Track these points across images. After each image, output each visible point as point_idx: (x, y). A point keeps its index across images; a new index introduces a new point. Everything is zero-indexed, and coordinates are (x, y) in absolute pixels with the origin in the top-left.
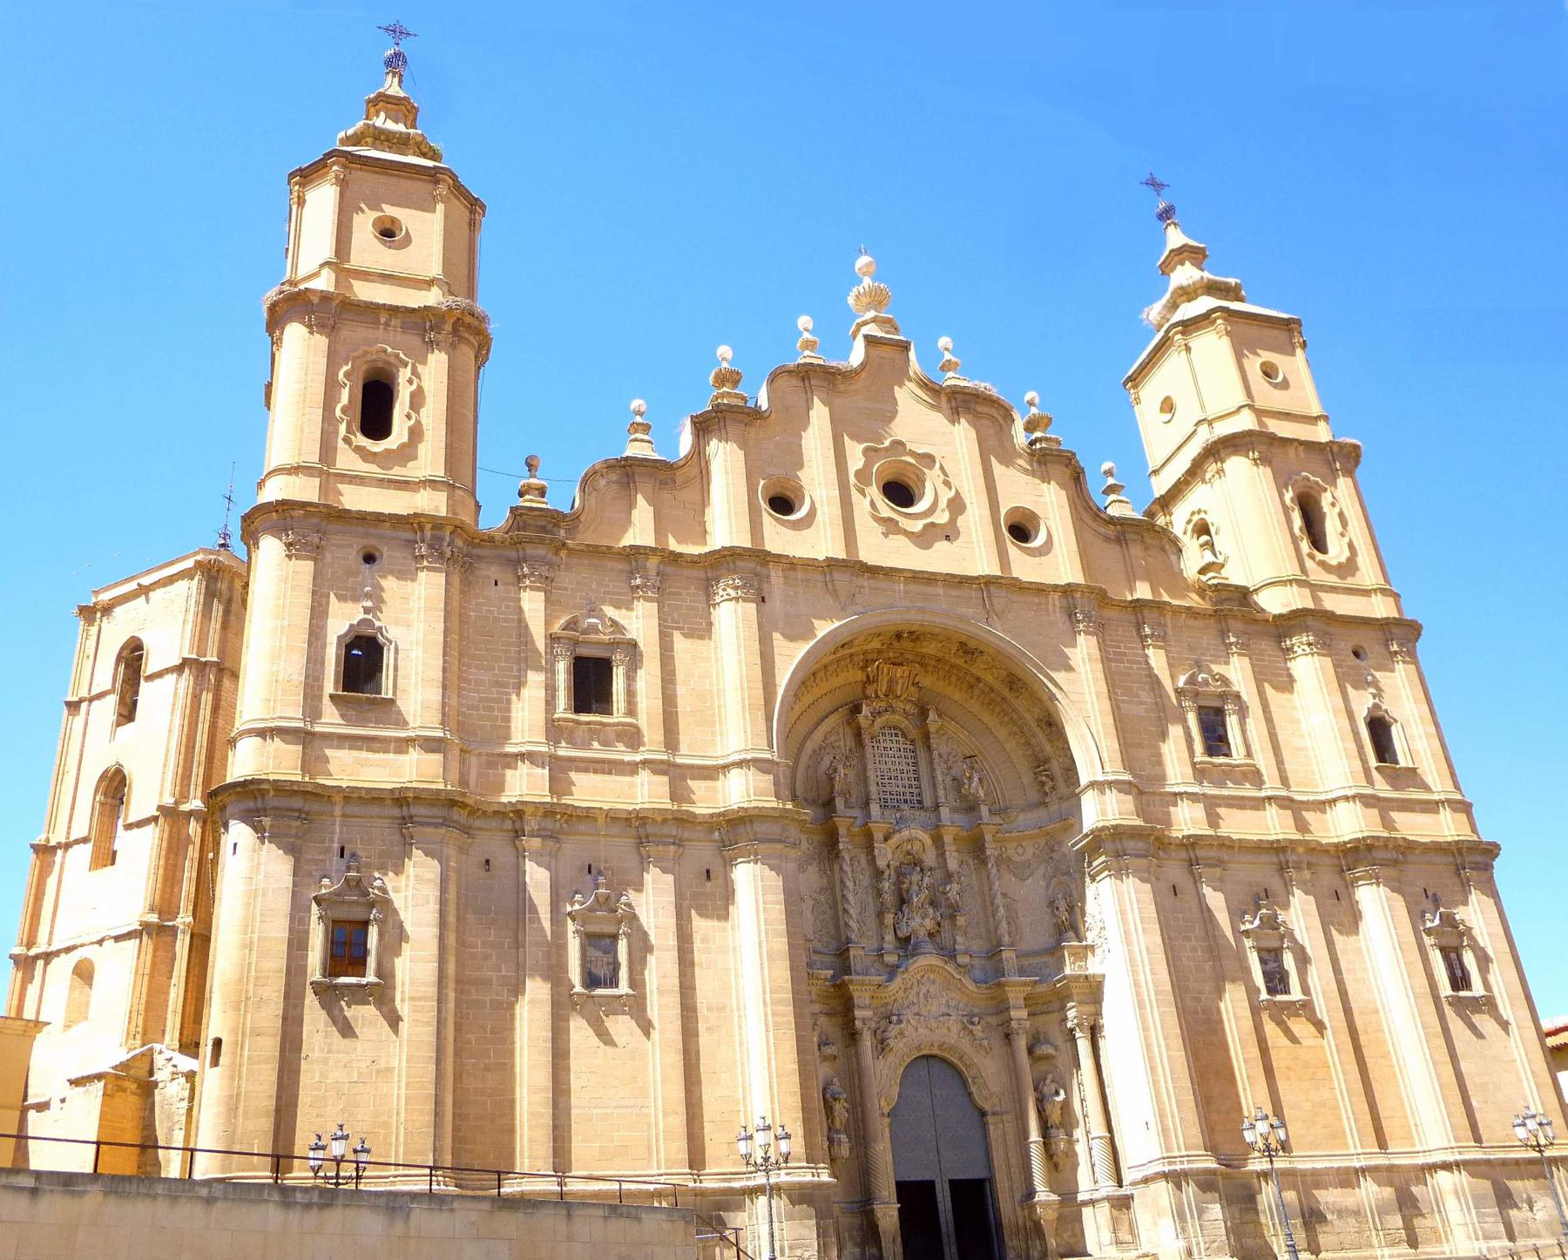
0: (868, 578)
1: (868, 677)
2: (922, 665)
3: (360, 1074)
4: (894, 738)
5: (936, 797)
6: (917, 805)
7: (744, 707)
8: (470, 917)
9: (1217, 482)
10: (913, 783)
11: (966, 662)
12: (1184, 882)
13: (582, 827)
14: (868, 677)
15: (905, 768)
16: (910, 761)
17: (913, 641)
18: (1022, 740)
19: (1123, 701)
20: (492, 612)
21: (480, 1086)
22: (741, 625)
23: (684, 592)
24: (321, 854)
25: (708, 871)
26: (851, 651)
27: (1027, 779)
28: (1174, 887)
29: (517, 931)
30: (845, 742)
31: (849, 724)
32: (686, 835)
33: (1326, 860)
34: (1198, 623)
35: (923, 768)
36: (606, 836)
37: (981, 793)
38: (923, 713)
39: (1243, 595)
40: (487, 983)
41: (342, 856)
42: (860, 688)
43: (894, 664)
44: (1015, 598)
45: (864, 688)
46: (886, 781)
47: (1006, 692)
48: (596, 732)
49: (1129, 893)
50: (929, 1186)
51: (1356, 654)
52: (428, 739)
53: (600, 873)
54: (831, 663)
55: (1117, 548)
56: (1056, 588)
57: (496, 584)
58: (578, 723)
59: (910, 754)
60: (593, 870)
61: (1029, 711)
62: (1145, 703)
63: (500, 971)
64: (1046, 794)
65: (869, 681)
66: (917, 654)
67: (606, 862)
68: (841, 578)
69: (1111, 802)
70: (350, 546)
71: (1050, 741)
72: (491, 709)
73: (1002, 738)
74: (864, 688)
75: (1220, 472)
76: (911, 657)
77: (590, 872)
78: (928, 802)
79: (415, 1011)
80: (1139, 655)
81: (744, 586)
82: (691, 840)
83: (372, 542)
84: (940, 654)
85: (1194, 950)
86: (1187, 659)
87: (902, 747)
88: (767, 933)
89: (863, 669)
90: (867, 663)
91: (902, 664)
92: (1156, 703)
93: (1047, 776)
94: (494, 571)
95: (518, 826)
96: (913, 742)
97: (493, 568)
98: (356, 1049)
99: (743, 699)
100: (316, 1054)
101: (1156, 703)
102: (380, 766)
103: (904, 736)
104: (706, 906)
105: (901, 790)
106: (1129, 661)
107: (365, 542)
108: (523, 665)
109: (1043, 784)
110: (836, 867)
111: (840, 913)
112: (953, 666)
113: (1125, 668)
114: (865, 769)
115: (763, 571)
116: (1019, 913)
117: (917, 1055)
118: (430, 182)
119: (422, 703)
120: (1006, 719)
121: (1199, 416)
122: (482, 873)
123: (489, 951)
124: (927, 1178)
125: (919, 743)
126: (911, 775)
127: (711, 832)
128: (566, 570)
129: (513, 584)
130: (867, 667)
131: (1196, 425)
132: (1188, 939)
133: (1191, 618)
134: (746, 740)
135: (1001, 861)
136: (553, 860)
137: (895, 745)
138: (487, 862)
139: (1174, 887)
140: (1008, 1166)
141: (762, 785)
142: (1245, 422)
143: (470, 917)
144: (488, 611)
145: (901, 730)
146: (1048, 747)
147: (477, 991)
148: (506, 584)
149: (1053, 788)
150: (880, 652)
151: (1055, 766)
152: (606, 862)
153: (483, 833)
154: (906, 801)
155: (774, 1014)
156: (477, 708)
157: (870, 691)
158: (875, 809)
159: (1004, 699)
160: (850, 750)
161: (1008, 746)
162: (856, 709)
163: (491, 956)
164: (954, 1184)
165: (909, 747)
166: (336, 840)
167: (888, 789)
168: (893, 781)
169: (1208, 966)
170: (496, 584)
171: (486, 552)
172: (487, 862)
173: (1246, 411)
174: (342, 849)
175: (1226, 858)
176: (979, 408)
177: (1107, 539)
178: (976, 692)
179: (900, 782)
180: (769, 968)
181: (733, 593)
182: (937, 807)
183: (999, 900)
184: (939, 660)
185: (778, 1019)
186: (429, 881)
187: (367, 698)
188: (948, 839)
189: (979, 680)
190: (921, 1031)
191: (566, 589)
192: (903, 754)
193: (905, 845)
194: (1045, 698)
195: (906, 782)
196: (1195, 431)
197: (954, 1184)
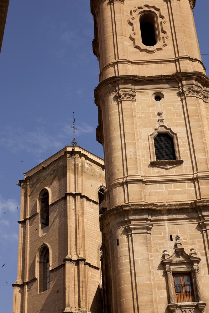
24: (160, 240)
41: (172, 240)
102: (182, 194)
166: (167, 232)
174: (171, 236)
187: (169, 162)
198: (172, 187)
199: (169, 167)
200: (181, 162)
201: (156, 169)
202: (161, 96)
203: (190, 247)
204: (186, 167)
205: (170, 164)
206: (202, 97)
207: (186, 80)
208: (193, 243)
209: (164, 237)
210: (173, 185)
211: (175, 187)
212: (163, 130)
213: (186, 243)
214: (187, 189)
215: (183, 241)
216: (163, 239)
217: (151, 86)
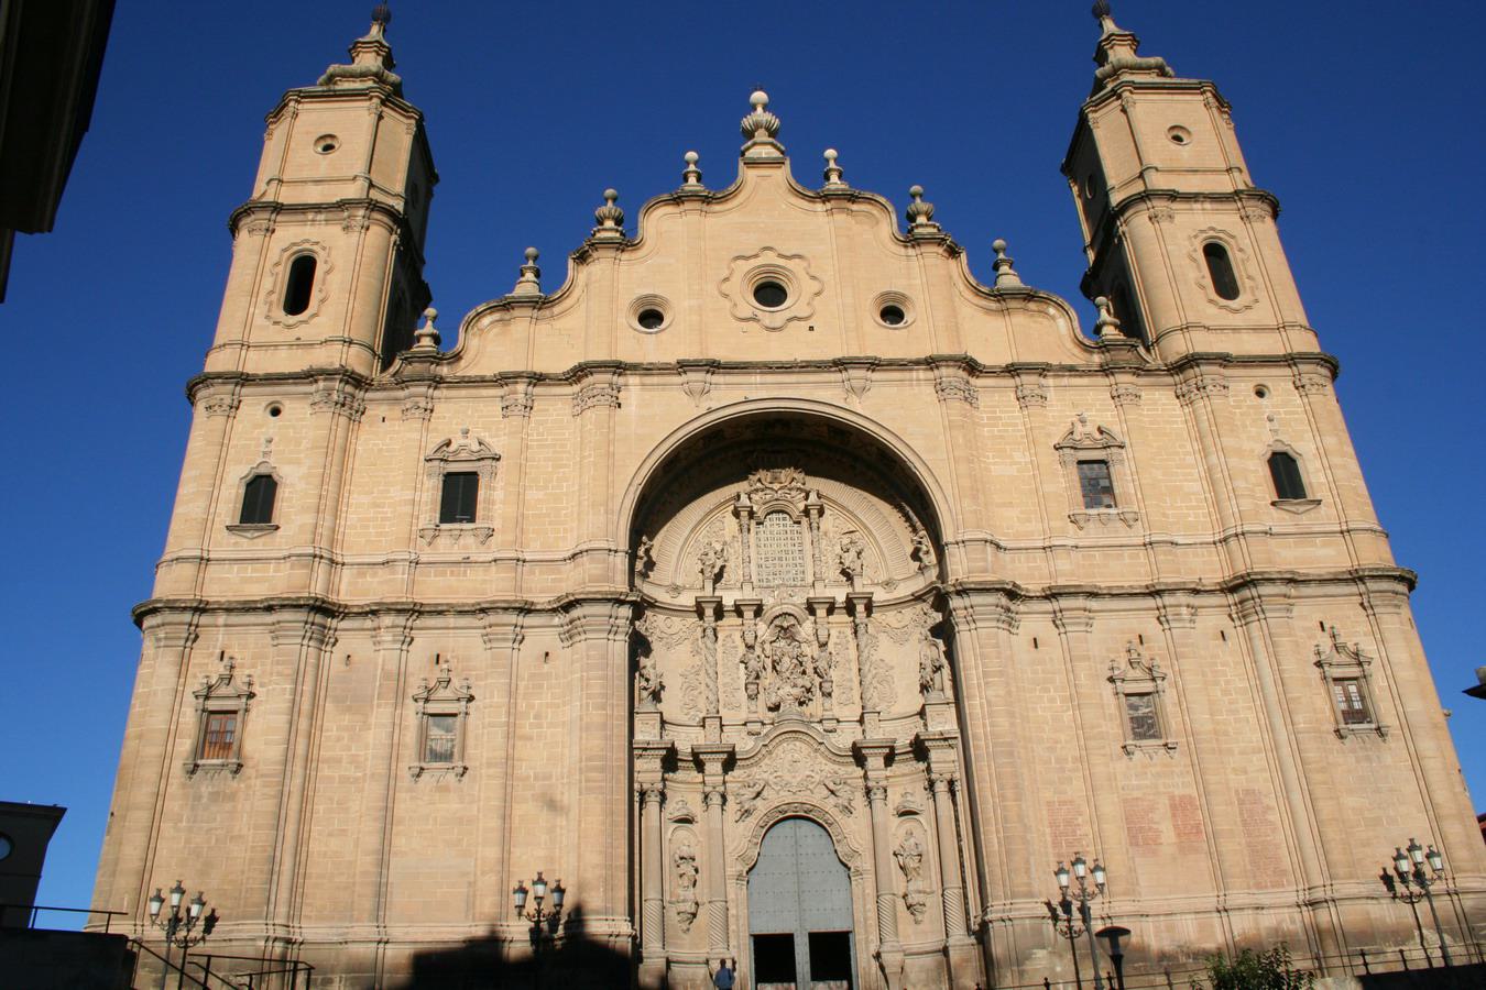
3: (217, 840)
4: (782, 522)
15: (790, 548)
19: (995, 464)
21: (324, 849)
23: (551, 408)
25: (547, 654)
28: (1035, 639)
34: (1085, 381)
40: (338, 761)
50: (786, 941)
51: (1260, 394)
56: (917, 363)
62: (1020, 463)
63: (350, 750)
70: (260, 404)
72: (367, 527)
79: (264, 786)
83: (278, 398)
85: (1052, 700)
88: (587, 704)
94: (382, 410)
98: (215, 819)
100: (184, 824)
104: (541, 686)
107: (271, 399)
113: (999, 431)
116: (895, 679)
117: (781, 816)
118: (366, 100)
122: (343, 667)
124: (787, 932)
126: (797, 554)
132: (1048, 691)
138: (349, 656)
139: (1035, 639)
140: (866, 919)
141: (594, 572)
144: (374, 445)
147: (329, 767)
155: (587, 781)
164: (816, 939)
169: (1068, 716)
174: (223, 653)
176: (855, 207)
177: (988, 311)
180: (587, 739)
185: (589, 784)
186: (288, 675)
190: (782, 793)
192: (789, 536)
193: (777, 622)
197: (816, 939)
198: (250, 570)
199: (256, 534)
200: (277, 528)
201: (234, 539)
203: (247, 672)
204: (281, 537)
207: (325, 380)
208: (253, 666)
209: (212, 655)
210: (250, 567)
211: (254, 571)
212: (263, 470)
213: (242, 666)
215: (239, 661)
216: (209, 657)
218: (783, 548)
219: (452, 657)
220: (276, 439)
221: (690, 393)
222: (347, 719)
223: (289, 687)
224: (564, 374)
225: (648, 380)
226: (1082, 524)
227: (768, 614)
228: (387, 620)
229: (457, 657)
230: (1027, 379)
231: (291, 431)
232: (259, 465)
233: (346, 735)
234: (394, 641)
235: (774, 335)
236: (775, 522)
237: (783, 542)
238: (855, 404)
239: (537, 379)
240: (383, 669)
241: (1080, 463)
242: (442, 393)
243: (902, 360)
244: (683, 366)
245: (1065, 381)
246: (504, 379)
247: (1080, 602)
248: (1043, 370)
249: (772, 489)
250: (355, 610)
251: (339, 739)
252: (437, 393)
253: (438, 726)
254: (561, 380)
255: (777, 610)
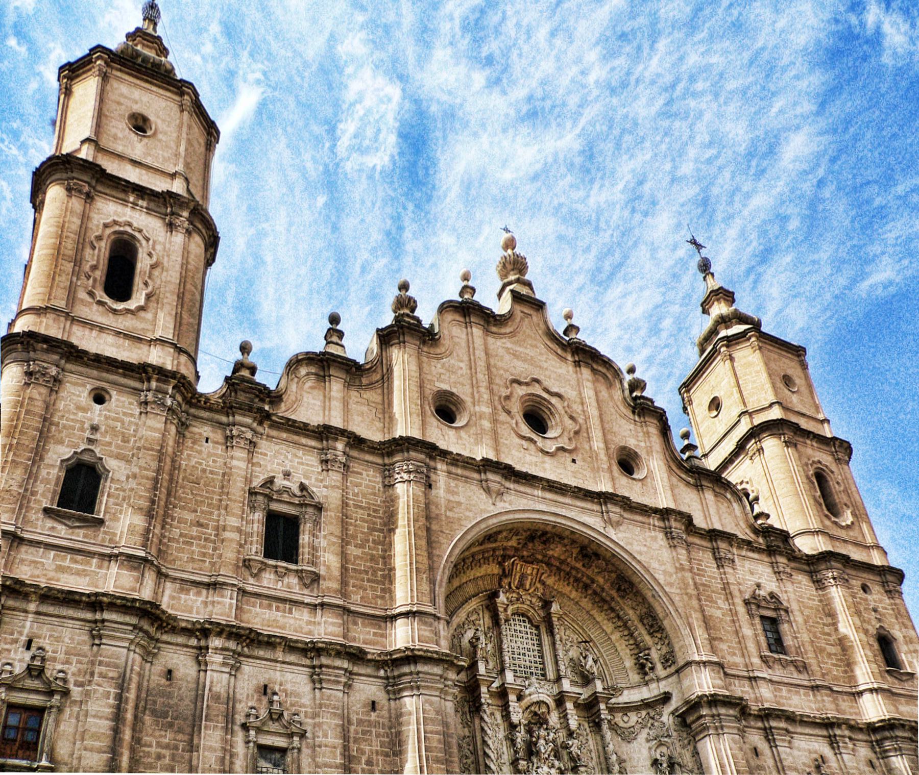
0: (515, 482)
1: (504, 570)
2: (548, 564)
5: (558, 670)
6: (541, 677)
7: (411, 569)
8: (148, 719)
9: (757, 459)
10: (538, 659)
11: (584, 566)
12: (763, 746)
13: (261, 653)
14: (504, 570)
16: (535, 642)
17: (544, 543)
18: (626, 633)
19: (706, 605)
20: (201, 464)
22: (411, 503)
23: (364, 473)
26: (494, 545)
27: (629, 663)
29: (192, 736)
30: (485, 620)
31: (487, 607)
32: (356, 669)
33: (861, 736)
35: (547, 648)
36: (283, 662)
37: (595, 669)
38: (547, 605)
39: (784, 536)
42: (496, 580)
43: (524, 561)
44: (626, 515)
45: (500, 580)
46: (516, 656)
47: (614, 593)
48: (280, 576)
49: (725, 750)
52: (130, 557)
53: (275, 693)
54: (478, 552)
55: (696, 492)
56: (656, 511)
57: (207, 441)
58: (266, 564)
59: (535, 638)
60: (269, 691)
61: (633, 608)
64: (646, 674)
65: (504, 574)
66: (545, 556)
67: (281, 685)
68: (493, 477)
69: (706, 678)
71: (651, 634)
73: (609, 631)
74: (500, 580)
75: (760, 450)
76: (540, 557)
77: (265, 693)
78: (551, 675)
80: (714, 573)
81: (416, 472)
82: (360, 675)
84: (562, 557)
86: (749, 580)
87: (529, 631)
89: (500, 564)
90: (505, 557)
91: (532, 563)
92: (731, 610)
93: (647, 659)
94: (205, 430)
95: (203, 643)
96: (537, 628)
97: (206, 428)
99: (411, 564)
101: (731, 610)
103: (530, 622)
105: (528, 664)
106: (709, 576)
108: (223, 512)
109: (642, 666)
110: (477, 721)
111: (481, 759)
112: (572, 568)
114: (500, 642)
115: (432, 464)
119: (130, 526)
120: (613, 615)
121: (742, 408)
123: (164, 751)
125: (543, 630)
126: (536, 653)
127: (378, 669)
128: (266, 440)
129: (221, 444)
130: (504, 562)
131: (739, 416)
133: (750, 550)
134: (412, 597)
135: (614, 727)
136: (233, 679)
137: (523, 629)
142: (776, 413)
143: (148, 719)
145: (528, 618)
146: (647, 638)
148: (217, 443)
149: (652, 669)
150: (516, 549)
151: (655, 655)
152: (281, 685)
153: (170, 647)
154: (532, 673)
156: (178, 542)
157: (505, 581)
158: (509, 677)
159: (613, 599)
160: (489, 628)
161: (613, 637)
162: (495, 595)
163: (165, 757)
165: (534, 631)
167: (517, 662)
168: (521, 657)
170: (207, 441)
171: (203, 414)
172: (170, 672)
173: (776, 408)
175: (791, 728)
178: (590, 592)
179: (527, 658)
181: (406, 476)
182: (558, 679)
183: (614, 758)
184: (562, 562)
188: (569, 705)
189: (593, 581)
191: (266, 455)
192: (529, 636)
193: (533, 709)
194: (649, 595)
195: (532, 659)
196: (739, 421)
202: (107, 397)
205: (79, 519)
206: (175, 422)
214: (93, 569)
217: (95, 373)
218: (525, 645)
219: (280, 690)
220: (103, 428)
221: (488, 491)
222: (168, 737)
223: (113, 691)
224: (381, 443)
225: (453, 469)
226: (771, 664)
227: (526, 702)
228: (216, 642)
229: (285, 691)
230: (723, 545)
231: (119, 424)
232: (83, 451)
233: (166, 752)
234: (224, 664)
235: (547, 459)
236: (517, 622)
237: (525, 641)
238: (611, 533)
239: (357, 442)
240: (210, 690)
241: (762, 618)
242: (266, 429)
243: (646, 506)
244: (487, 465)
245: (744, 553)
246: (325, 433)
247: (782, 725)
248: (729, 537)
249: (518, 593)
250: (183, 625)
251: (159, 757)
252: (260, 429)
253: (265, 759)
254: (376, 449)
255: (535, 698)
